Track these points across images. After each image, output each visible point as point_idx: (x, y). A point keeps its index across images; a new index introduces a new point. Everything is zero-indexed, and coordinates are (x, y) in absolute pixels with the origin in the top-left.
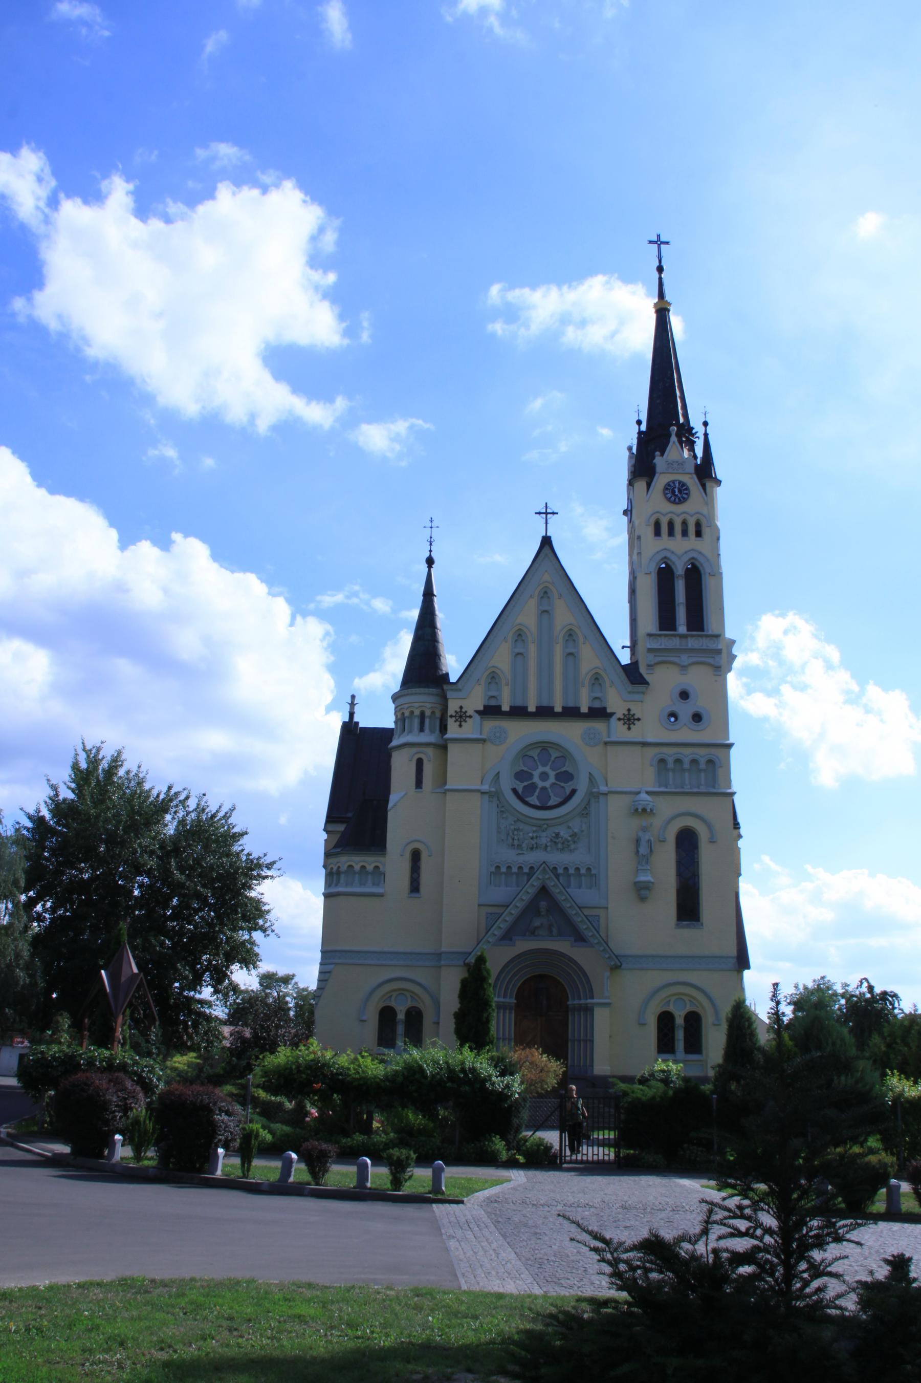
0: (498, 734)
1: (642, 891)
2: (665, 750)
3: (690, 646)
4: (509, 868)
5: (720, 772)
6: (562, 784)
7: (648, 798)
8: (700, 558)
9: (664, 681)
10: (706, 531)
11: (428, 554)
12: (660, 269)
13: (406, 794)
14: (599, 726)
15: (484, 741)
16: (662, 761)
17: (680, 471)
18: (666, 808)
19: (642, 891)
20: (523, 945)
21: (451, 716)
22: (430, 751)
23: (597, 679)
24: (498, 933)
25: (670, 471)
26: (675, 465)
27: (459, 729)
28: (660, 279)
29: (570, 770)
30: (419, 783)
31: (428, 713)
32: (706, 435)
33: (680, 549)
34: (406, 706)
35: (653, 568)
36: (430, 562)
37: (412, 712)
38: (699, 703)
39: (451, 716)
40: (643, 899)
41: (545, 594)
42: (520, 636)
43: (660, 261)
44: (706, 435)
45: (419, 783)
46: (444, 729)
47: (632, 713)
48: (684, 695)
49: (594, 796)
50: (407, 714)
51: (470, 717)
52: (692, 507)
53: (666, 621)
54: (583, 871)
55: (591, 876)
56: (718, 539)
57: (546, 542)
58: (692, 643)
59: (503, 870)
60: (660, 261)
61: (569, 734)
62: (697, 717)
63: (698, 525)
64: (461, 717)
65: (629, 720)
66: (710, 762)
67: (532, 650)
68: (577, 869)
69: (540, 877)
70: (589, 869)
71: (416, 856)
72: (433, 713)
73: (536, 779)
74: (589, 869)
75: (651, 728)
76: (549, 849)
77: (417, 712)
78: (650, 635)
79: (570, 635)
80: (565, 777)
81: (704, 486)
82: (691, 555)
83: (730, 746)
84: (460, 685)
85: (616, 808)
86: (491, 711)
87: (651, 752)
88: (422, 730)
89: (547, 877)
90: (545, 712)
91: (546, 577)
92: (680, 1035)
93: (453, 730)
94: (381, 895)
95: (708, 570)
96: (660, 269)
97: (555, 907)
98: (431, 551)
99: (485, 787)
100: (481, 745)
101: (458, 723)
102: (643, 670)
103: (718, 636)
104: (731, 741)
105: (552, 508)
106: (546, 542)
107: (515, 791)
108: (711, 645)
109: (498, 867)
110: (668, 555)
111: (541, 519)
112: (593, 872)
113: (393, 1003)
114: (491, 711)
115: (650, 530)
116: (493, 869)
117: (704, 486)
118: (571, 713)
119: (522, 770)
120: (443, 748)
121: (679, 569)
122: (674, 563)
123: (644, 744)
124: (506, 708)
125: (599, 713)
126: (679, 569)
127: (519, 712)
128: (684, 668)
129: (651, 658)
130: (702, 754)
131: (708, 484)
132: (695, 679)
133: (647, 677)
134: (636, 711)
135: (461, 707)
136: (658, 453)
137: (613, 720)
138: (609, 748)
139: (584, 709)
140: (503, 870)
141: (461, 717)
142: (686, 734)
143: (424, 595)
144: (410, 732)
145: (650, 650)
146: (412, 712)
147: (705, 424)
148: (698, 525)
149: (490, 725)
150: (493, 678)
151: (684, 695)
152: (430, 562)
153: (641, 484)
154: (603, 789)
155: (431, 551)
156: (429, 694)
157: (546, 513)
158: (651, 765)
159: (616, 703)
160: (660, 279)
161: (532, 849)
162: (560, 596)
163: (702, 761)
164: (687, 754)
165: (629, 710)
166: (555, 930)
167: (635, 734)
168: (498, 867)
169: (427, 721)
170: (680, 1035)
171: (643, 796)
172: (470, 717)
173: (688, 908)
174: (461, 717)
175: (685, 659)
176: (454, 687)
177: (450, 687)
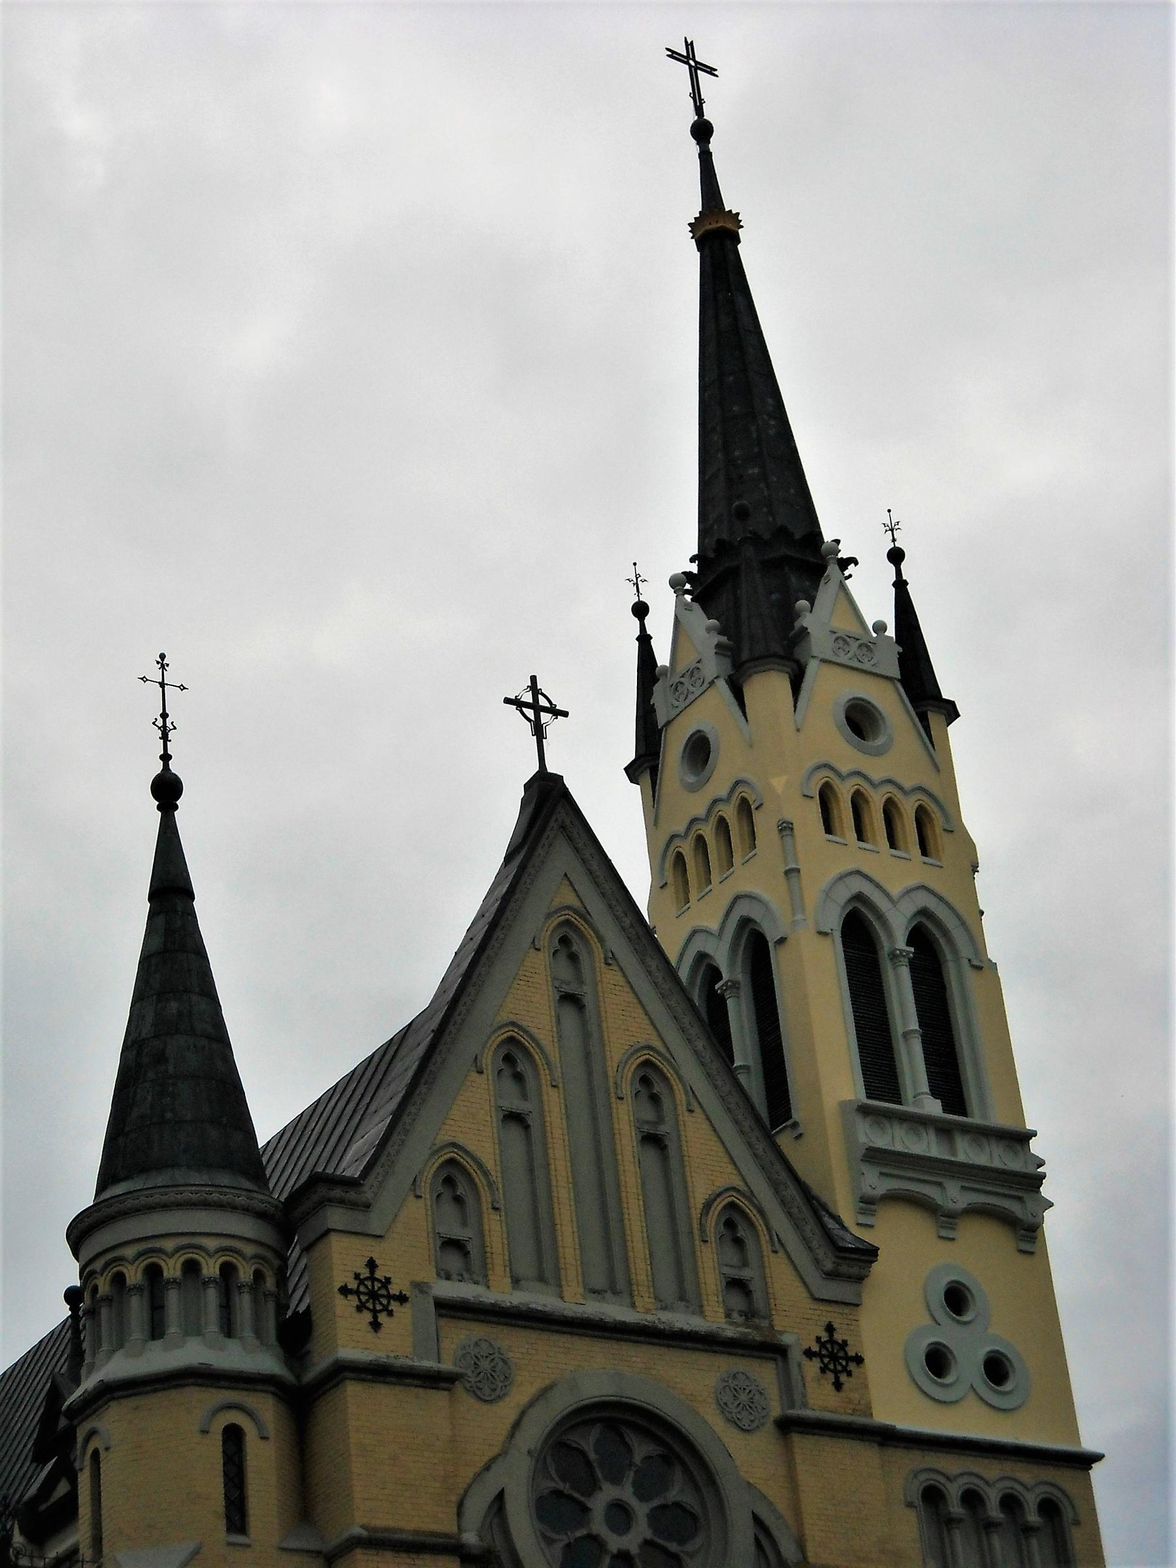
0: (485, 1365)
3: (961, 1158)
5: (1077, 1539)
6: (673, 1547)
11: (158, 767)
12: (702, 131)
13: (196, 1552)
17: (867, 666)
21: (345, 1291)
22: (267, 1407)
23: (734, 1223)
25: (843, 659)
26: (854, 645)
27: (370, 1336)
28: (706, 158)
29: (689, 1499)
30: (236, 1515)
31: (245, 1273)
32: (900, 585)
34: (169, 1245)
35: (834, 921)
36: (167, 790)
37: (191, 1268)
38: (998, 1324)
39: (345, 1291)
42: (514, 1055)
43: (699, 110)
44: (900, 585)
45: (236, 1515)
46: (295, 1334)
47: (838, 1337)
48: (956, 1299)
50: (172, 1269)
51: (402, 1299)
56: (975, 869)
58: (966, 1152)
60: (699, 110)
62: (996, 1369)
64: (374, 1295)
66: (1049, 1508)
72: (258, 1275)
77: (211, 1268)
78: (864, 1111)
79: (650, 1078)
82: (923, 900)
83: (1085, 1461)
84: (367, 1193)
88: (228, 1329)
95: (965, 951)
96: (702, 131)
98: (166, 758)
100: (446, 1393)
101: (367, 1316)
103: (1023, 1138)
104: (1088, 1443)
105: (554, 691)
108: (1014, 1164)
111: (519, 726)
117: (923, 718)
119: (557, 1493)
120: (304, 1399)
122: (880, 917)
123: (887, 1437)
126: (895, 935)
128: (945, 1219)
129: (875, 1182)
130: (1030, 1482)
131: (934, 719)
132: (977, 1254)
135: (372, 1265)
136: (803, 603)
143: (155, 895)
144: (193, 1329)
145: (874, 1156)
146: (191, 1268)
147: (896, 556)
148: (922, 818)
151: (956, 1299)
152: (167, 790)
155: (166, 758)
156: (246, 1210)
158: (910, 1505)
160: (706, 158)
162: (611, 959)
164: (993, 1476)
165: (830, 1329)
169: (244, 1303)
172: (402, 1299)
174: (374, 1295)
175: (954, 1196)
176: (352, 1195)
177: (337, 1192)
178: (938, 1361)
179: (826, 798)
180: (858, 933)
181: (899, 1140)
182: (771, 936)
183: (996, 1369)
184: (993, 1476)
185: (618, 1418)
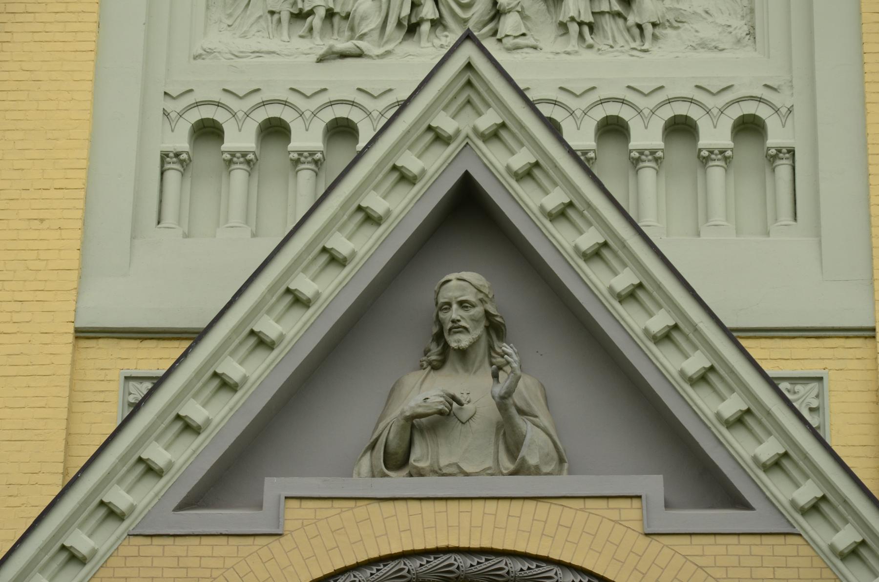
4: (275, 131)
24: (183, 459)
54: (715, 134)
59: (240, 137)
68: (681, 128)
69: (446, 123)
70: (749, 127)
74: (749, 127)
76: (509, 24)
89: (488, 120)
109: (208, 131)
112: (777, 136)
116: (180, 140)
140: (240, 137)
161: (412, 29)
166: (536, 445)
168: (208, 131)
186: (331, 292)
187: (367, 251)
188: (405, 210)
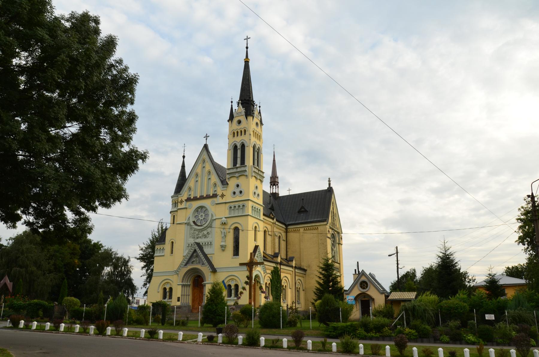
1: (223, 248)
2: (231, 204)
7: (225, 219)
8: (244, 142)
9: (232, 183)
10: (247, 132)
12: (247, 48)
14: (215, 199)
15: (186, 208)
16: (231, 207)
18: (230, 221)
19: (223, 248)
20: (190, 267)
28: (247, 51)
33: (238, 140)
36: (184, 157)
40: (223, 250)
41: (204, 161)
48: (238, 186)
49: (213, 220)
52: (242, 126)
53: (235, 163)
55: (210, 244)
57: (206, 147)
61: (206, 203)
62: (241, 192)
63: (245, 131)
65: (223, 196)
66: (243, 206)
67: (199, 179)
71: (173, 243)
73: (200, 217)
75: (229, 198)
79: (209, 172)
80: (207, 215)
81: (247, 118)
85: (217, 224)
86: (189, 200)
87: (228, 205)
90: (202, 198)
91: (204, 157)
92: (233, 292)
93: (180, 206)
94: (163, 256)
96: (247, 48)
97: (197, 256)
99: (185, 222)
102: (227, 180)
106: (206, 147)
107: (194, 222)
110: (235, 142)
113: (165, 286)
114: (189, 200)
115: (232, 135)
117: (247, 118)
118: (208, 197)
121: (239, 146)
123: (226, 203)
124: (192, 198)
125: (215, 196)
126: (239, 146)
127: (195, 199)
128: (237, 177)
131: (248, 118)
133: (228, 182)
134: (225, 193)
137: (218, 197)
138: (217, 206)
139: (211, 195)
141: (181, 202)
142: (238, 198)
145: (228, 174)
148: (245, 131)
149: (188, 203)
150: (190, 189)
151: (238, 186)
152: (184, 157)
153: (230, 122)
154: (214, 218)
157: (207, 137)
159: (219, 192)
160: (247, 51)
163: (241, 206)
164: (237, 204)
167: (224, 200)
170: (233, 292)
171: (224, 219)
173: (236, 252)
175: (237, 175)
178: (234, 193)
179: (234, 133)
180: (235, 147)
181: (235, 170)
182: (246, 145)
183: (241, 192)
184: (237, 204)
185: (201, 207)
186: (189, 255)
187: (191, 253)
188: (192, 251)
